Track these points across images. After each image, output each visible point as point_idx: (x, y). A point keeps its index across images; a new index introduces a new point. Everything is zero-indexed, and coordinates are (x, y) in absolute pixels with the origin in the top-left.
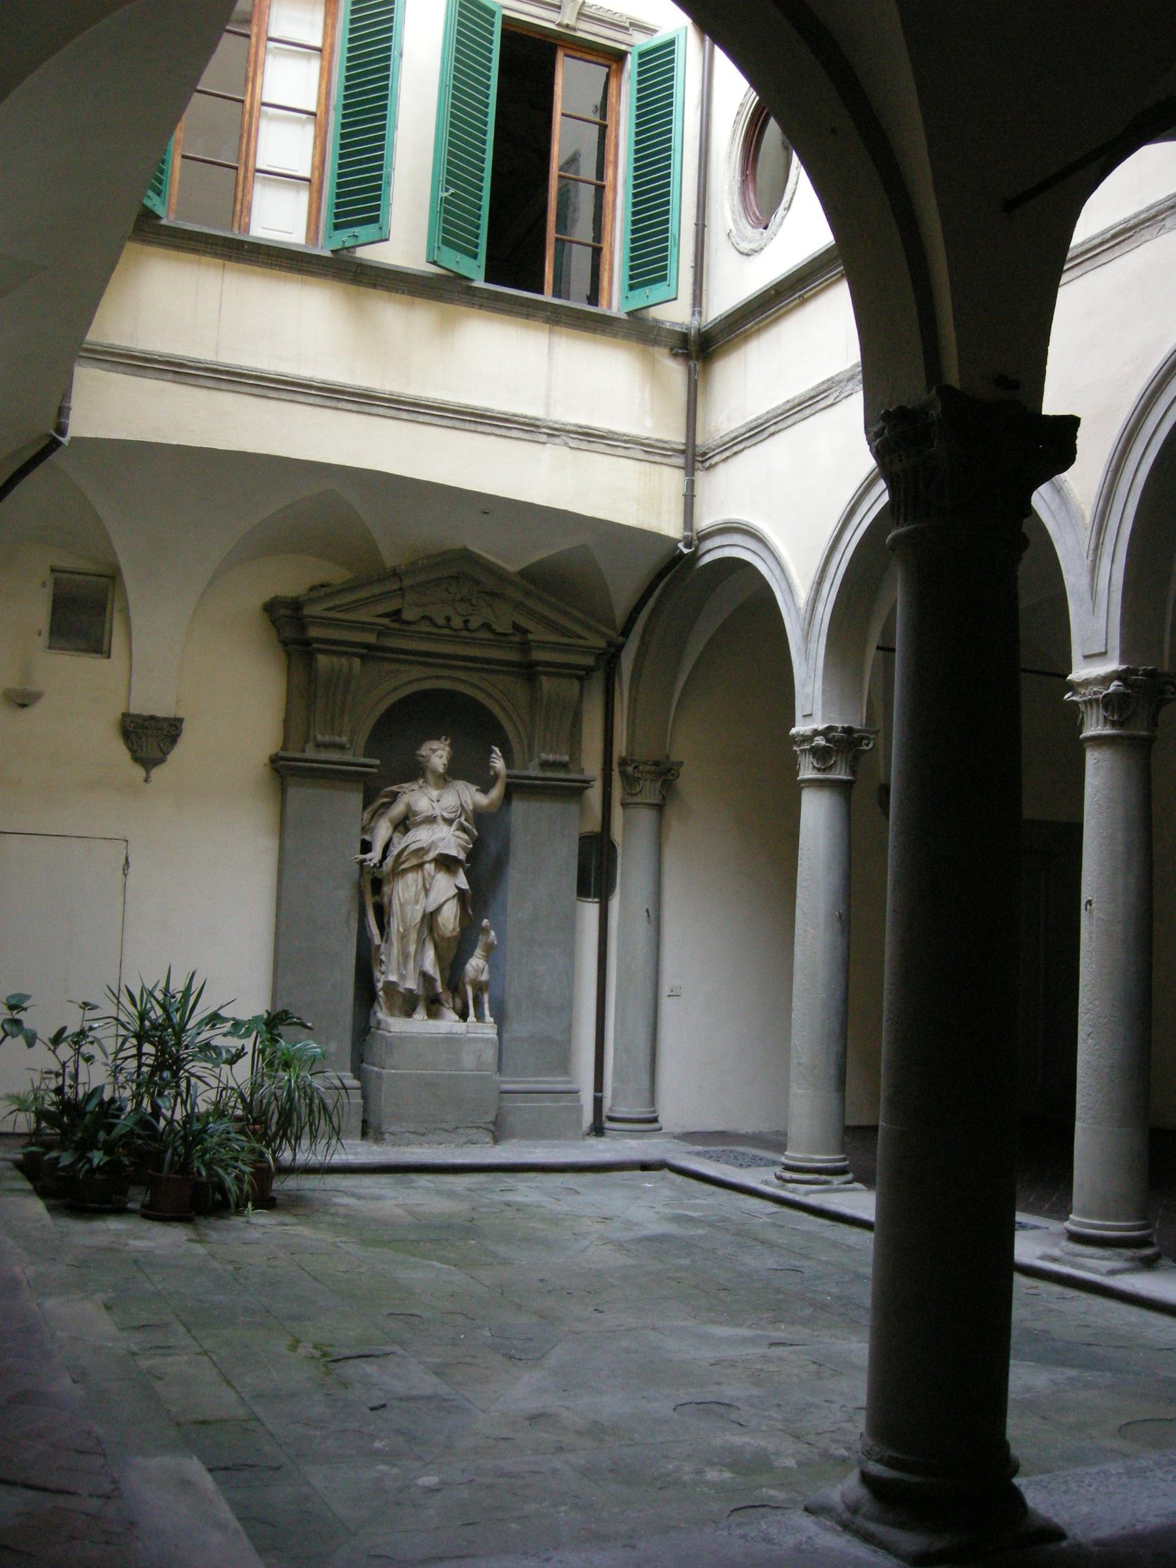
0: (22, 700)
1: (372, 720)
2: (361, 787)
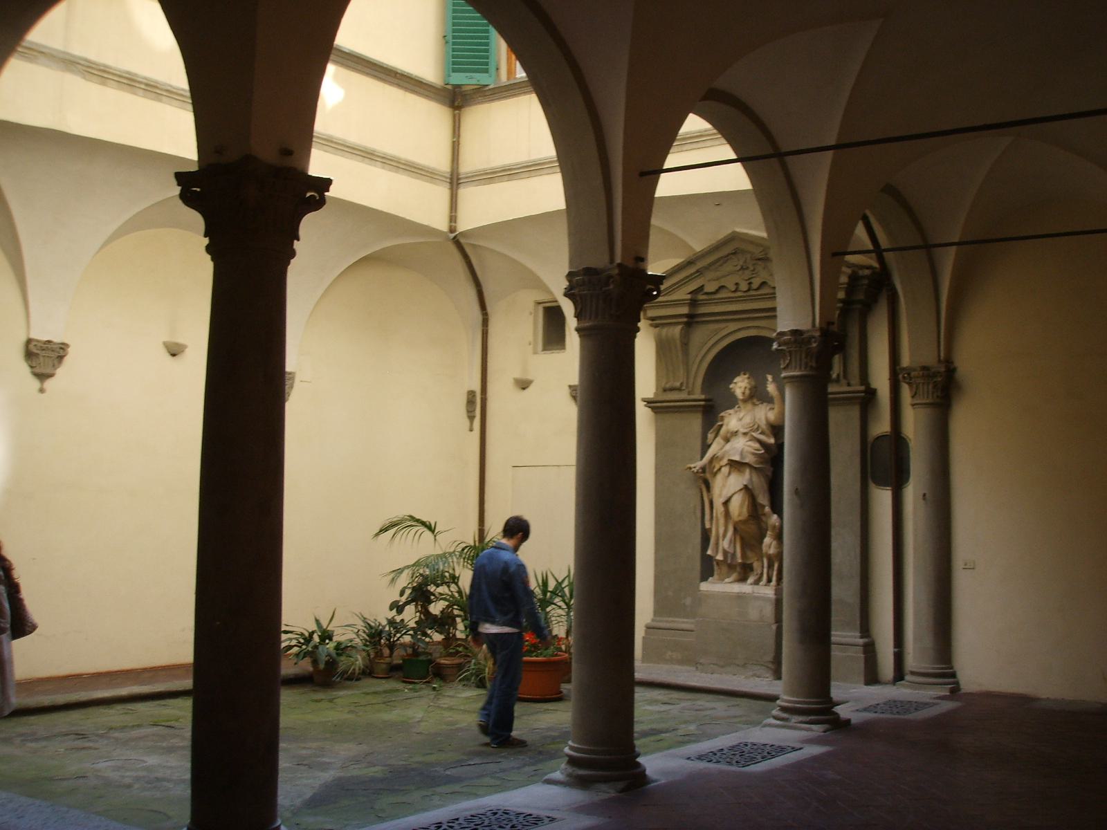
0: (523, 385)
1: (705, 365)
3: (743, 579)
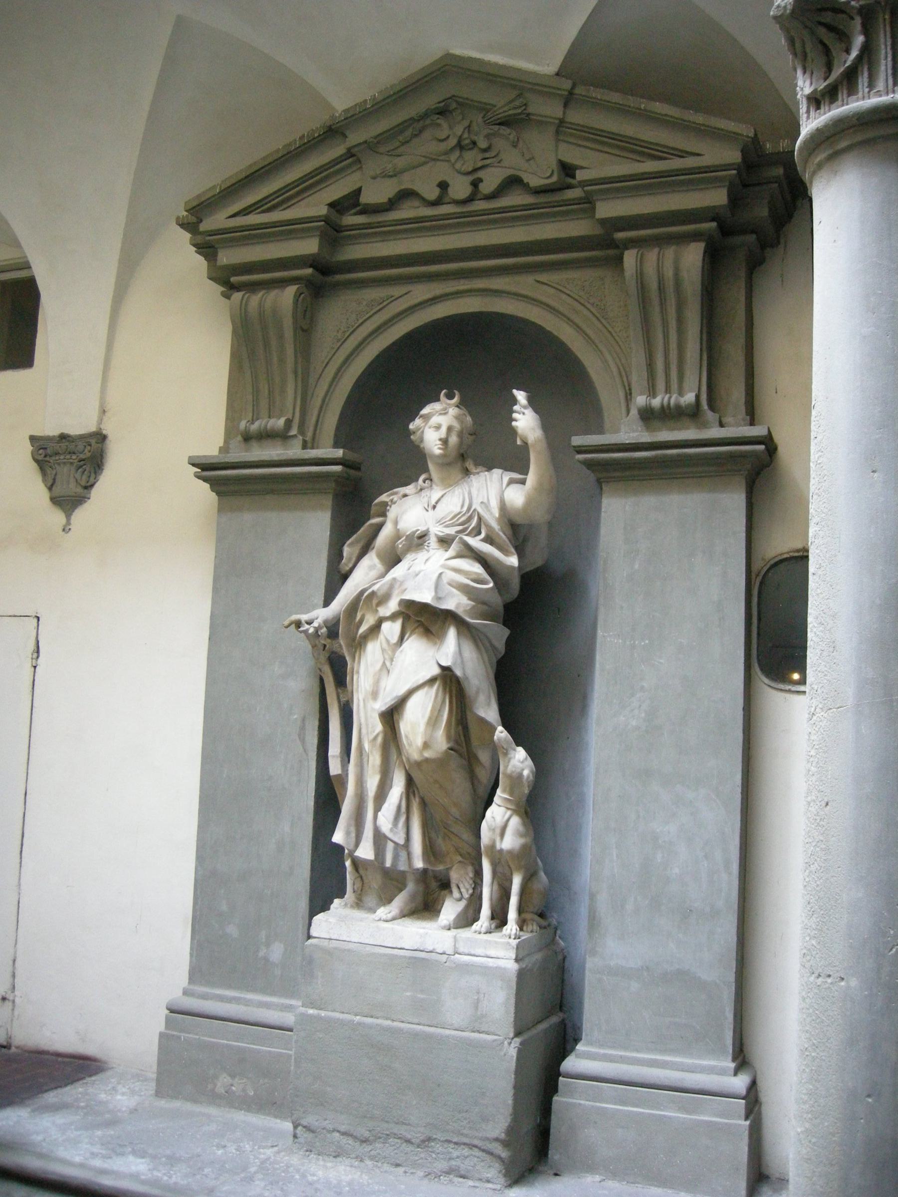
2: (328, 501)
3: (426, 907)
